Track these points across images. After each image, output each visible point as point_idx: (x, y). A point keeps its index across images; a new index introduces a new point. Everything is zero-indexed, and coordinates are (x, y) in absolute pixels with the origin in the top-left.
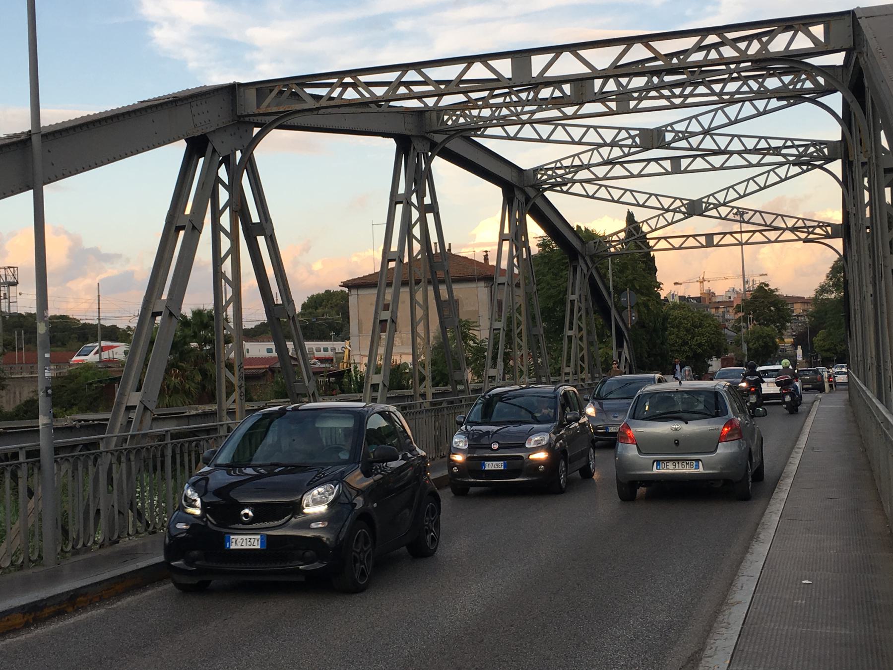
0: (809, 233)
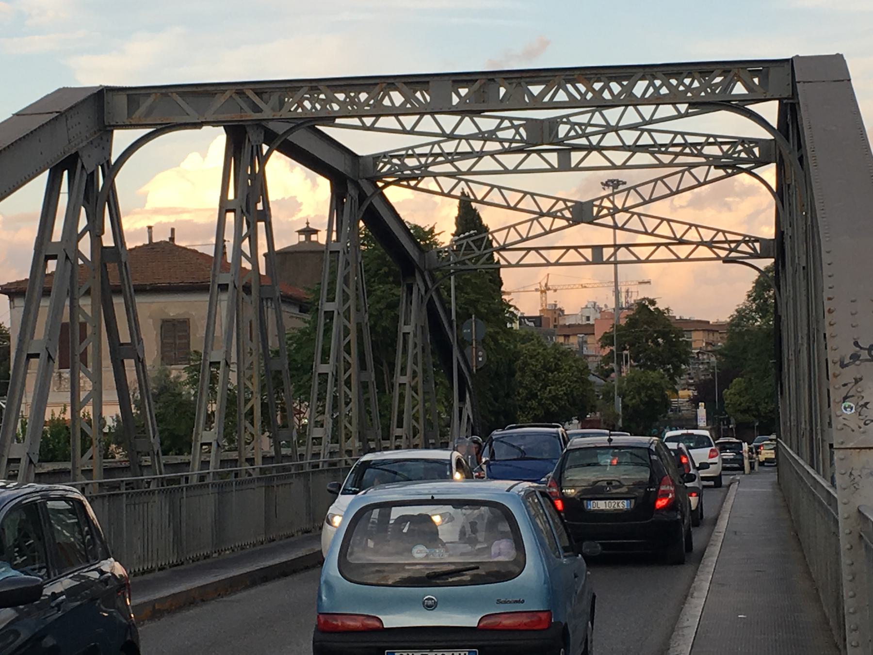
0: (731, 250)
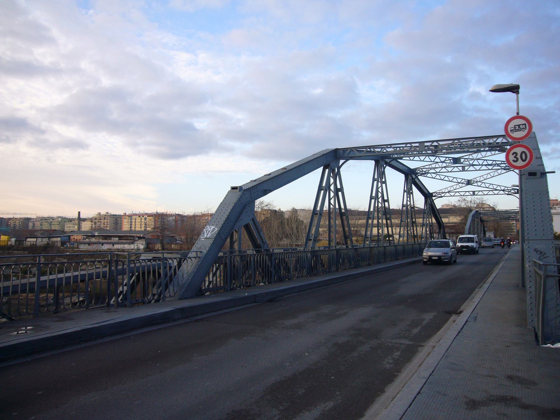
0: (509, 192)
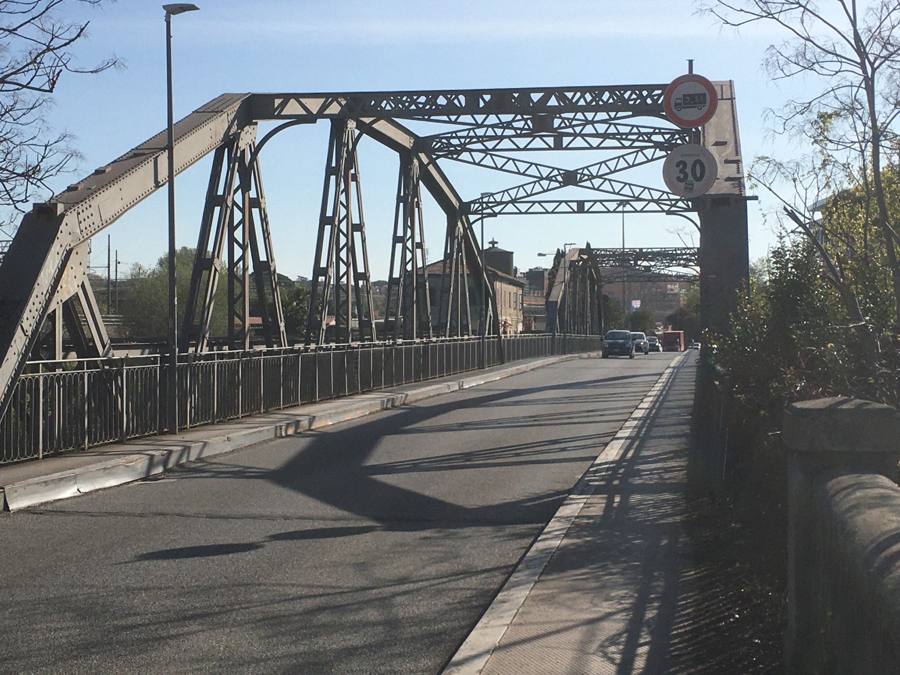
0: (672, 206)
